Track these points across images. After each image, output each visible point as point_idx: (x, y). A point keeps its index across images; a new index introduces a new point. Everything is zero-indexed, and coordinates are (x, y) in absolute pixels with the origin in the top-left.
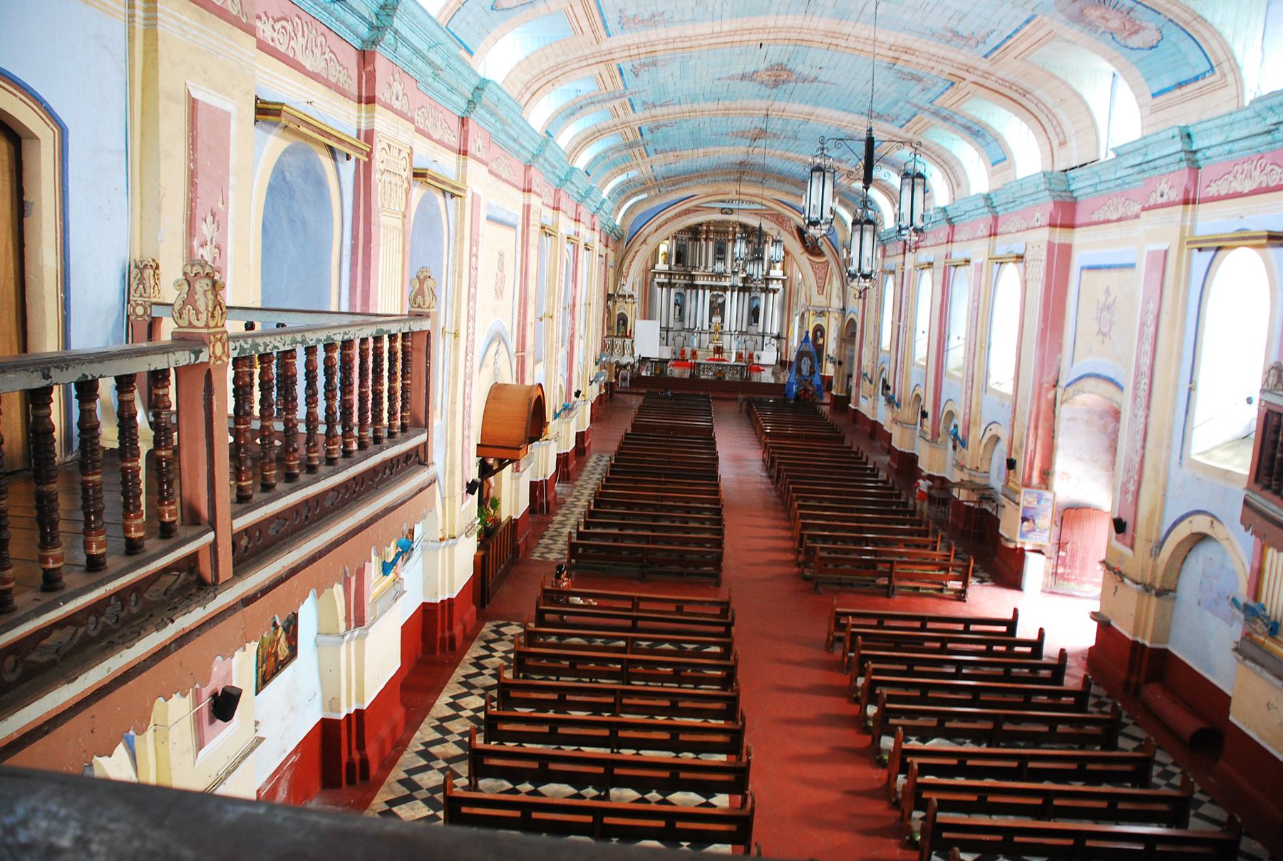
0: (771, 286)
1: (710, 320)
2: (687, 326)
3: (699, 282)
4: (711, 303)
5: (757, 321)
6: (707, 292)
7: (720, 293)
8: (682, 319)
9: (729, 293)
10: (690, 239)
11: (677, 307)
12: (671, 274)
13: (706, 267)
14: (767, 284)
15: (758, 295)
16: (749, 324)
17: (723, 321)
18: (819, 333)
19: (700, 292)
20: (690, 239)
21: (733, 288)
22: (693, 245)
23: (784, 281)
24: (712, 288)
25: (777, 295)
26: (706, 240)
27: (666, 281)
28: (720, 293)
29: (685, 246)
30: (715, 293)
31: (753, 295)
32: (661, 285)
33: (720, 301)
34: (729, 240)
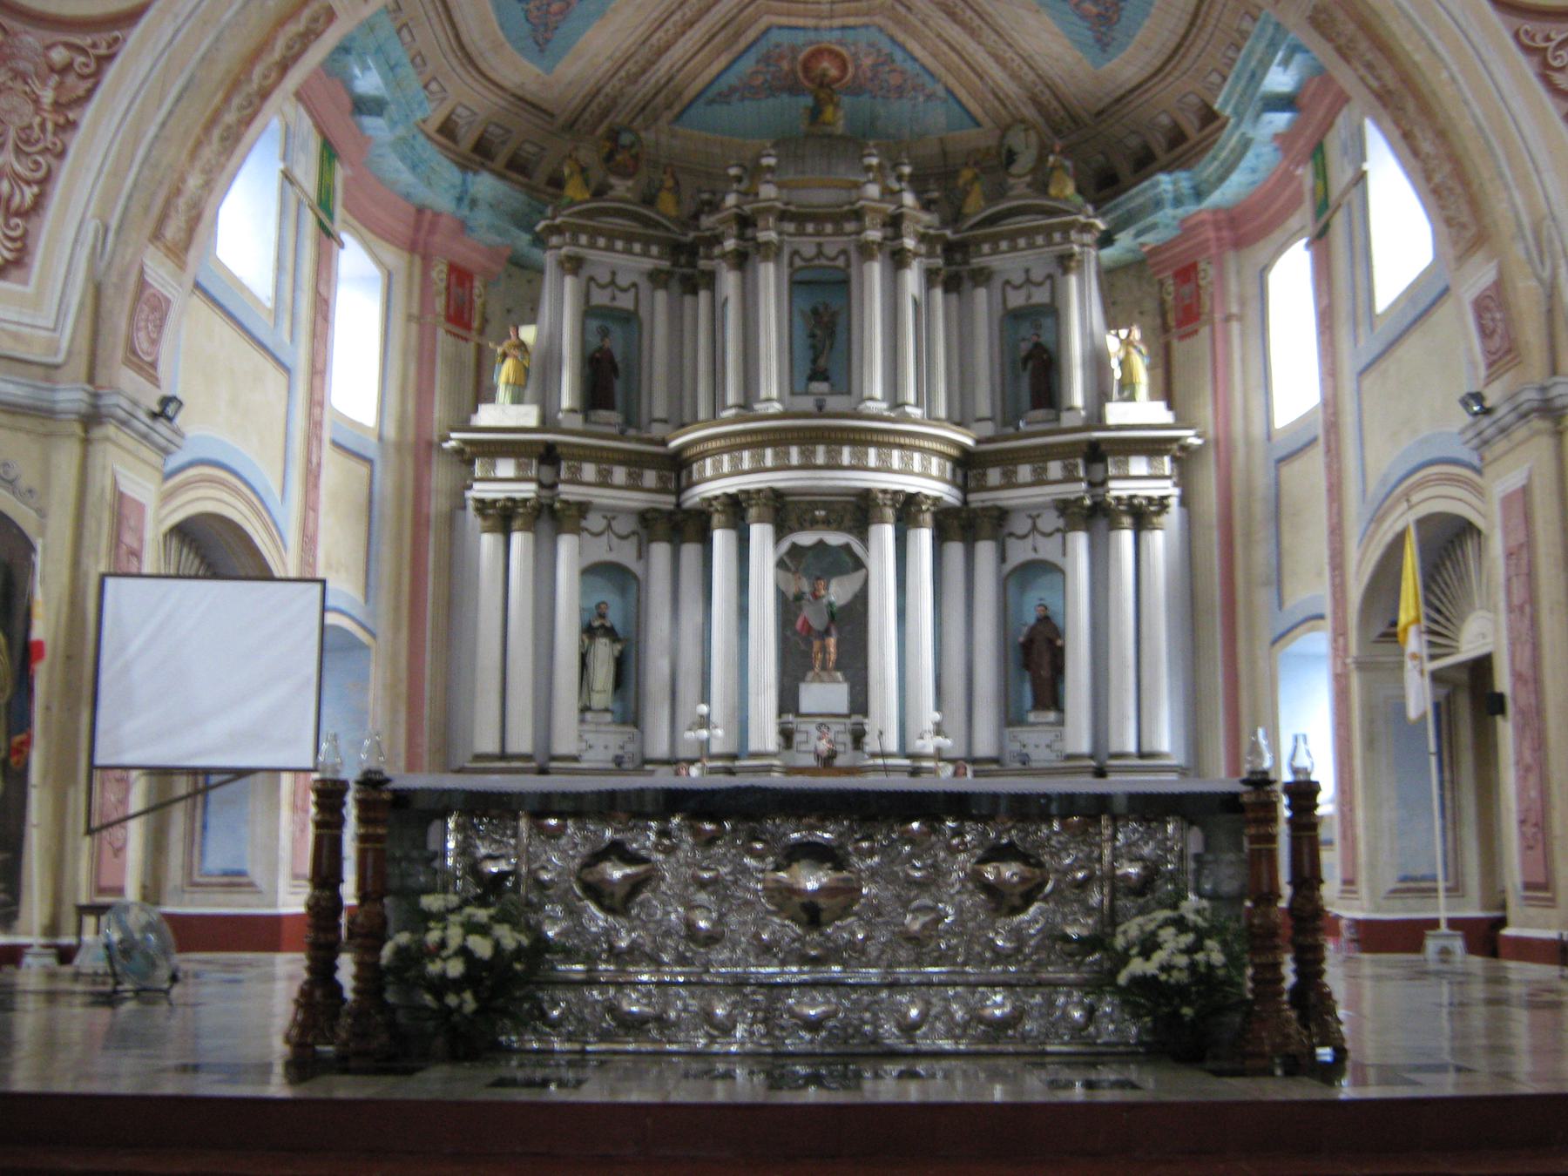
1: (788, 702)
4: (788, 607)
5: (1050, 696)
6: (761, 534)
7: (835, 539)
9: (885, 534)
10: (657, 279)
11: (604, 652)
13: (746, 405)
14: (1098, 484)
15: (1047, 550)
16: (1010, 718)
17: (860, 703)
19: (722, 540)
20: (657, 279)
21: (907, 509)
22: (676, 318)
23: (1185, 459)
25: (1160, 542)
26: (741, 260)
27: (527, 490)
28: (835, 539)
29: (629, 319)
30: (806, 538)
31: (1020, 553)
32: (503, 517)
33: (838, 592)
34: (866, 251)
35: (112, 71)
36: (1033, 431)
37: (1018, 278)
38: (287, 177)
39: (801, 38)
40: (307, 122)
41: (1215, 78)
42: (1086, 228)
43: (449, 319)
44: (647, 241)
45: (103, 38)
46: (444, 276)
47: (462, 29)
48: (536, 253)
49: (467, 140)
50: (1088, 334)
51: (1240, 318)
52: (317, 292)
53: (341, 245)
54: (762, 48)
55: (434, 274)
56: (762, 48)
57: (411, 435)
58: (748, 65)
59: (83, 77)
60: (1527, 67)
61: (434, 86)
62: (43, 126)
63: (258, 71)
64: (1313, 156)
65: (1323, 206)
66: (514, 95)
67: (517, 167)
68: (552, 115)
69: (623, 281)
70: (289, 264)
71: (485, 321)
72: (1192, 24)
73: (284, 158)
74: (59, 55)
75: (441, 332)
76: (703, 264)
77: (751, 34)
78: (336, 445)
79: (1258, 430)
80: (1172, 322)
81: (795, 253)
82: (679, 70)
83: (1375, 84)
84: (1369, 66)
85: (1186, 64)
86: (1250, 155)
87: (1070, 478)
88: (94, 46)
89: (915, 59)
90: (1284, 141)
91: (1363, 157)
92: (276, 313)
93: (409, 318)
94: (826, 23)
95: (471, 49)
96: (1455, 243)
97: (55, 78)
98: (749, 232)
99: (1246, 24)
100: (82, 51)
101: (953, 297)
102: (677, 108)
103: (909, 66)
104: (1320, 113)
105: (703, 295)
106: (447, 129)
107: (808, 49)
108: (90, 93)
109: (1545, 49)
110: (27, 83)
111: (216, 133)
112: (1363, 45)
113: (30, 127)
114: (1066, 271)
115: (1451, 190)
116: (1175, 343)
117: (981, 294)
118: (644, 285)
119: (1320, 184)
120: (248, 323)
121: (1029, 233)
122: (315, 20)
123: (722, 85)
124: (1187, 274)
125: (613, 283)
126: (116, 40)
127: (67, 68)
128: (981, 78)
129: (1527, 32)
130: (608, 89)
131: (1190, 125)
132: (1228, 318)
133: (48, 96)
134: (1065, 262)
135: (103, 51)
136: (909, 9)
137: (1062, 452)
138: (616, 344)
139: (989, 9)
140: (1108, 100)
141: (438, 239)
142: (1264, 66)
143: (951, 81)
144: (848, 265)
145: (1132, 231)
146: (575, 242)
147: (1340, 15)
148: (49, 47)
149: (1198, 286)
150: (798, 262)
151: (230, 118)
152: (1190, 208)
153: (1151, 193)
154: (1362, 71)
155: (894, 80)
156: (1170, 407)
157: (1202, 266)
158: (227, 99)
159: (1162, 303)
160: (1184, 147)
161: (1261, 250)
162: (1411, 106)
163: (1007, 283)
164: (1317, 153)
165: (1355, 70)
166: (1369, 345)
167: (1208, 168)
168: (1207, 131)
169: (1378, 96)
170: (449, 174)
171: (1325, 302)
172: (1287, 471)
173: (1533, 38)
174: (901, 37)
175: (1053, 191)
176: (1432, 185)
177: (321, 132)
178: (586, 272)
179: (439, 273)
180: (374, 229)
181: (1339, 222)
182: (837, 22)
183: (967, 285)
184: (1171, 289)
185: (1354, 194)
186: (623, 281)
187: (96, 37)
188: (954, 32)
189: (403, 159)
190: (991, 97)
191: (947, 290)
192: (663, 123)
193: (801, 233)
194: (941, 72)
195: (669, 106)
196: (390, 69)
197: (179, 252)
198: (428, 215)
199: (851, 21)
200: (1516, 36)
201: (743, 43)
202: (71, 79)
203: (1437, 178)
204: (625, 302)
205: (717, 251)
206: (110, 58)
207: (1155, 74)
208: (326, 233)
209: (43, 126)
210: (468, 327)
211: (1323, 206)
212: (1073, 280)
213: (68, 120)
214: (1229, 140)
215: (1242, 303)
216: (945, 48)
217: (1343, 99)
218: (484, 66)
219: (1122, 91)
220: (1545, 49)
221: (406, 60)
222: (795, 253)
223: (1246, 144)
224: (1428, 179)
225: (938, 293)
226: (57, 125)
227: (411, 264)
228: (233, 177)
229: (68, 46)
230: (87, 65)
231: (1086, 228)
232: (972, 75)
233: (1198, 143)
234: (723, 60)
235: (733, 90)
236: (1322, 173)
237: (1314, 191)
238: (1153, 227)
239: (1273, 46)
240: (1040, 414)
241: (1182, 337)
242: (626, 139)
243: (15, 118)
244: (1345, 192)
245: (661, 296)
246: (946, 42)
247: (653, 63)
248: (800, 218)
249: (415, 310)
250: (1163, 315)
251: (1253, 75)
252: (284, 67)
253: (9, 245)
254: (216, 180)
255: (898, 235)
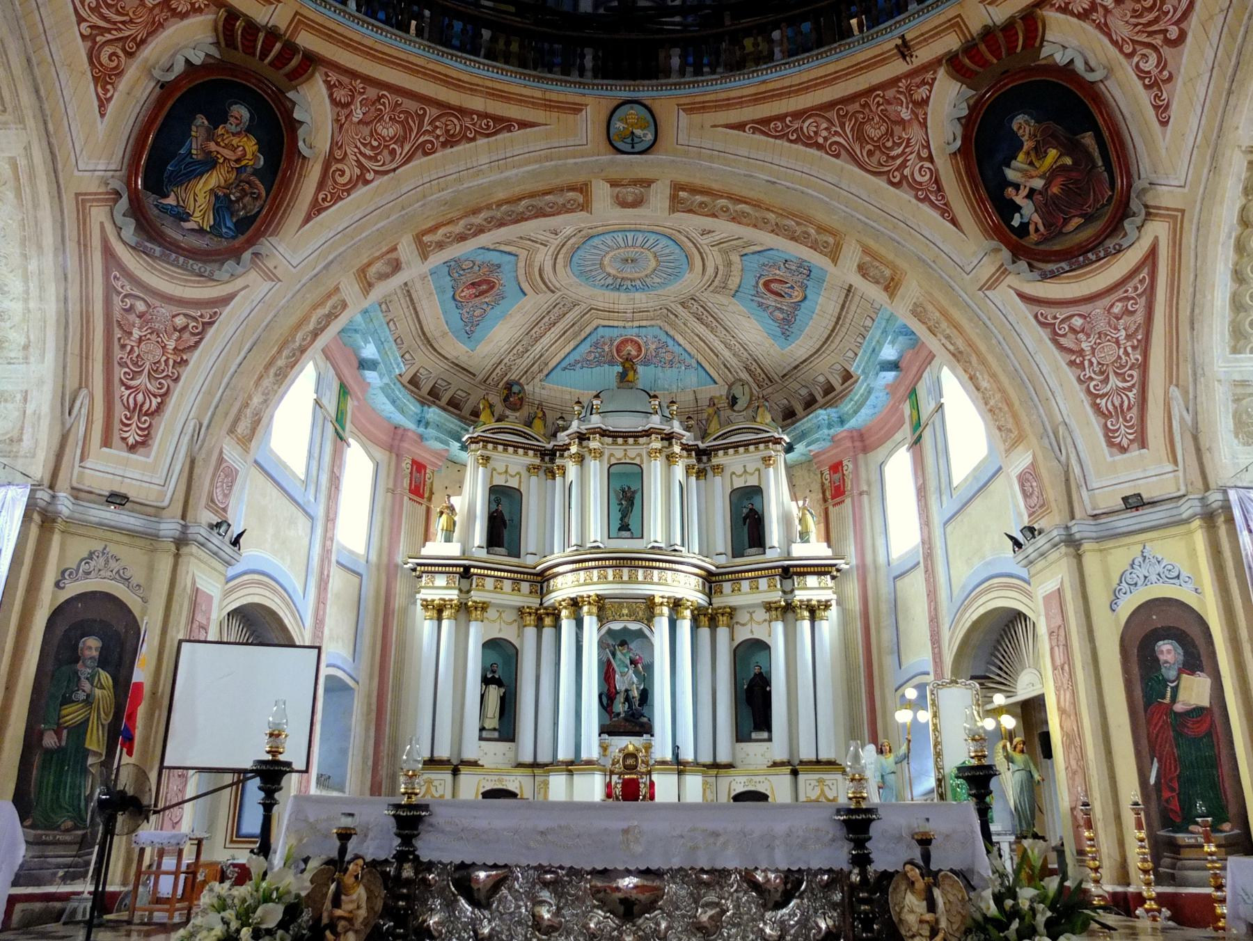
0: (800, 596)
2: (527, 758)
3: (565, 587)
8: (506, 728)
10: (532, 469)
12: (466, 573)
18: (1168, 651)
21: (676, 604)
24: (602, 605)
26: (580, 459)
35: (212, 331)
36: (751, 559)
37: (739, 471)
38: (317, 403)
39: (616, 332)
40: (332, 372)
41: (850, 354)
42: (777, 441)
43: (411, 491)
44: (526, 448)
45: (207, 312)
46: (409, 466)
47: (424, 323)
48: (464, 456)
49: (426, 389)
50: (781, 504)
51: (868, 493)
52: (333, 472)
53: (349, 445)
54: (593, 338)
55: (404, 465)
56: (593, 338)
57: (385, 559)
58: (585, 347)
59: (193, 334)
60: (1044, 334)
61: (407, 356)
62: (166, 361)
63: (299, 336)
64: (909, 396)
65: (917, 425)
66: (453, 363)
67: (454, 405)
68: (474, 375)
69: (512, 471)
70: (316, 455)
71: (432, 493)
72: (837, 323)
73: (317, 392)
74: (180, 321)
75: (406, 499)
76: (558, 461)
77: (588, 330)
78: (338, 562)
79: (882, 559)
80: (828, 494)
81: (612, 455)
82: (547, 350)
83: (951, 348)
84: (948, 337)
85: (833, 346)
86: (872, 397)
87: (771, 587)
88: (201, 316)
89: (680, 345)
90: (892, 389)
91: (941, 396)
92: (306, 483)
93: (388, 490)
94: (630, 324)
95: (429, 335)
96: (1005, 441)
97: (177, 334)
98: (585, 443)
99: (868, 323)
100: (194, 319)
101: (702, 481)
102: (545, 372)
103: (677, 349)
104: (914, 370)
105: (558, 479)
106: (414, 382)
107: (619, 340)
108: (197, 344)
109: (1054, 324)
110: (159, 337)
111: (272, 371)
112: (944, 325)
113: (159, 362)
114: (769, 466)
115: (1000, 409)
116: (831, 508)
117: (718, 479)
118: (524, 473)
119: (915, 413)
120: (284, 484)
121: (746, 445)
122: (335, 307)
123: (571, 359)
124: (836, 467)
125: (506, 472)
126: (216, 313)
127: (186, 327)
128: (717, 356)
129: (1042, 314)
130: (504, 361)
131: (836, 381)
132: (861, 494)
133: (171, 345)
134: (766, 460)
135: (206, 320)
136: (676, 316)
137: (767, 571)
138: (505, 508)
139: (722, 316)
140: (789, 368)
141: (405, 445)
142: (880, 344)
143: (700, 358)
144: (642, 461)
145: (804, 443)
146: (485, 447)
147: (930, 308)
148: (174, 316)
149: (843, 475)
150: (613, 461)
151: (280, 363)
152: (839, 429)
153: (815, 421)
154: (944, 341)
155: (668, 357)
156: (829, 546)
157: (845, 463)
158: (279, 352)
159: (823, 485)
160: (833, 395)
161: (880, 453)
162: (974, 359)
163: (734, 473)
164: (913, 393)
165: (940, 340)
166: (950, 506)
167: (846, 407)
168: (846, 384)
169: (953, 355)
170: (413, 407)
171: (921, 482)
172: (899, 583)
173: (1046, 318)
174: (672, 332)
175: (758, 419)
176: (988, 407)
177: (337, 375)
178: (492, 464)
179: (406, 465)
180: (369, 439)
181: (927, 435)
182: (636, 324)
183: (710, 473)
184: (828, 477)
185: (937, 417)
186: (512, 471)
187: (203, 311)
188: (701, 329)
189: (387, 397)
190: (722, 366)
191: (698, 478)
192: (537, 380)
193: (615, 443)
194: (694, 352)
195: (541, 371)
196: (380, 345)
197: (245, 442)
198: (400, 431)
199: (644, 323)
200: (1036, 317)
201: (583, 335)
202: (186, 335)
203: (992, 402)
204: (513, 483)
205: (566, 454)
206: (211, 324)
207: (815, 353)
208: (340, 437)
209: (166, 361)
210: (422, 496)
211: (917, 425)
212: (771, 470)
213: (182, 359)
214: (860, 389)
215: (869, 485)
216: (697, 339)
217: (931, 357)
218: (436, 346)
219: (797, 363)
220: (1054, 324)
221: (391, 339)
222: (612, 455)
223: (870, 391)
224: (986, 404)
225: (693, 479)
226: (175, 362)
227: (390, 458)
228: (282, 398)
229: (185, 315)
230: (197, 328)
231: (777, 441)
232: (712, 354)
233: (841, 392)
234: (572, 345)
235: (577, 362)
236: (916, 407)
237: (911, 415)
238: (817, 440)
239: (885, 332)
240: (753, 550)
241: (834, 505)
242: (515, 389)
243: (150, 357)
244: (932, 415)
245: (534, 479)
246: (698, 335)
247: (532, 346)
248: (614, 435)
249: (391, 486)
250: (824, 493)
251: (874, 350)
252: (315, 334)
253: (140, 433)
254: (271, 398)
255: (671, 444)
